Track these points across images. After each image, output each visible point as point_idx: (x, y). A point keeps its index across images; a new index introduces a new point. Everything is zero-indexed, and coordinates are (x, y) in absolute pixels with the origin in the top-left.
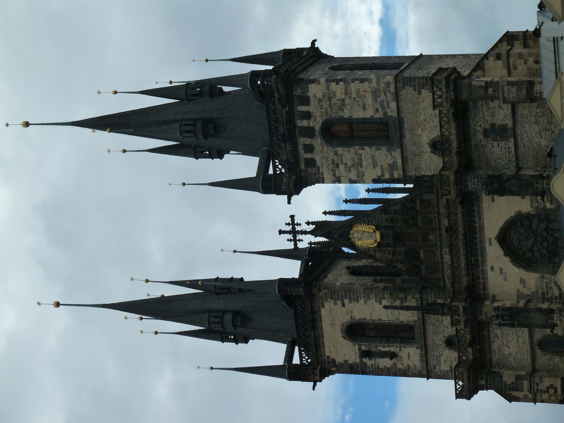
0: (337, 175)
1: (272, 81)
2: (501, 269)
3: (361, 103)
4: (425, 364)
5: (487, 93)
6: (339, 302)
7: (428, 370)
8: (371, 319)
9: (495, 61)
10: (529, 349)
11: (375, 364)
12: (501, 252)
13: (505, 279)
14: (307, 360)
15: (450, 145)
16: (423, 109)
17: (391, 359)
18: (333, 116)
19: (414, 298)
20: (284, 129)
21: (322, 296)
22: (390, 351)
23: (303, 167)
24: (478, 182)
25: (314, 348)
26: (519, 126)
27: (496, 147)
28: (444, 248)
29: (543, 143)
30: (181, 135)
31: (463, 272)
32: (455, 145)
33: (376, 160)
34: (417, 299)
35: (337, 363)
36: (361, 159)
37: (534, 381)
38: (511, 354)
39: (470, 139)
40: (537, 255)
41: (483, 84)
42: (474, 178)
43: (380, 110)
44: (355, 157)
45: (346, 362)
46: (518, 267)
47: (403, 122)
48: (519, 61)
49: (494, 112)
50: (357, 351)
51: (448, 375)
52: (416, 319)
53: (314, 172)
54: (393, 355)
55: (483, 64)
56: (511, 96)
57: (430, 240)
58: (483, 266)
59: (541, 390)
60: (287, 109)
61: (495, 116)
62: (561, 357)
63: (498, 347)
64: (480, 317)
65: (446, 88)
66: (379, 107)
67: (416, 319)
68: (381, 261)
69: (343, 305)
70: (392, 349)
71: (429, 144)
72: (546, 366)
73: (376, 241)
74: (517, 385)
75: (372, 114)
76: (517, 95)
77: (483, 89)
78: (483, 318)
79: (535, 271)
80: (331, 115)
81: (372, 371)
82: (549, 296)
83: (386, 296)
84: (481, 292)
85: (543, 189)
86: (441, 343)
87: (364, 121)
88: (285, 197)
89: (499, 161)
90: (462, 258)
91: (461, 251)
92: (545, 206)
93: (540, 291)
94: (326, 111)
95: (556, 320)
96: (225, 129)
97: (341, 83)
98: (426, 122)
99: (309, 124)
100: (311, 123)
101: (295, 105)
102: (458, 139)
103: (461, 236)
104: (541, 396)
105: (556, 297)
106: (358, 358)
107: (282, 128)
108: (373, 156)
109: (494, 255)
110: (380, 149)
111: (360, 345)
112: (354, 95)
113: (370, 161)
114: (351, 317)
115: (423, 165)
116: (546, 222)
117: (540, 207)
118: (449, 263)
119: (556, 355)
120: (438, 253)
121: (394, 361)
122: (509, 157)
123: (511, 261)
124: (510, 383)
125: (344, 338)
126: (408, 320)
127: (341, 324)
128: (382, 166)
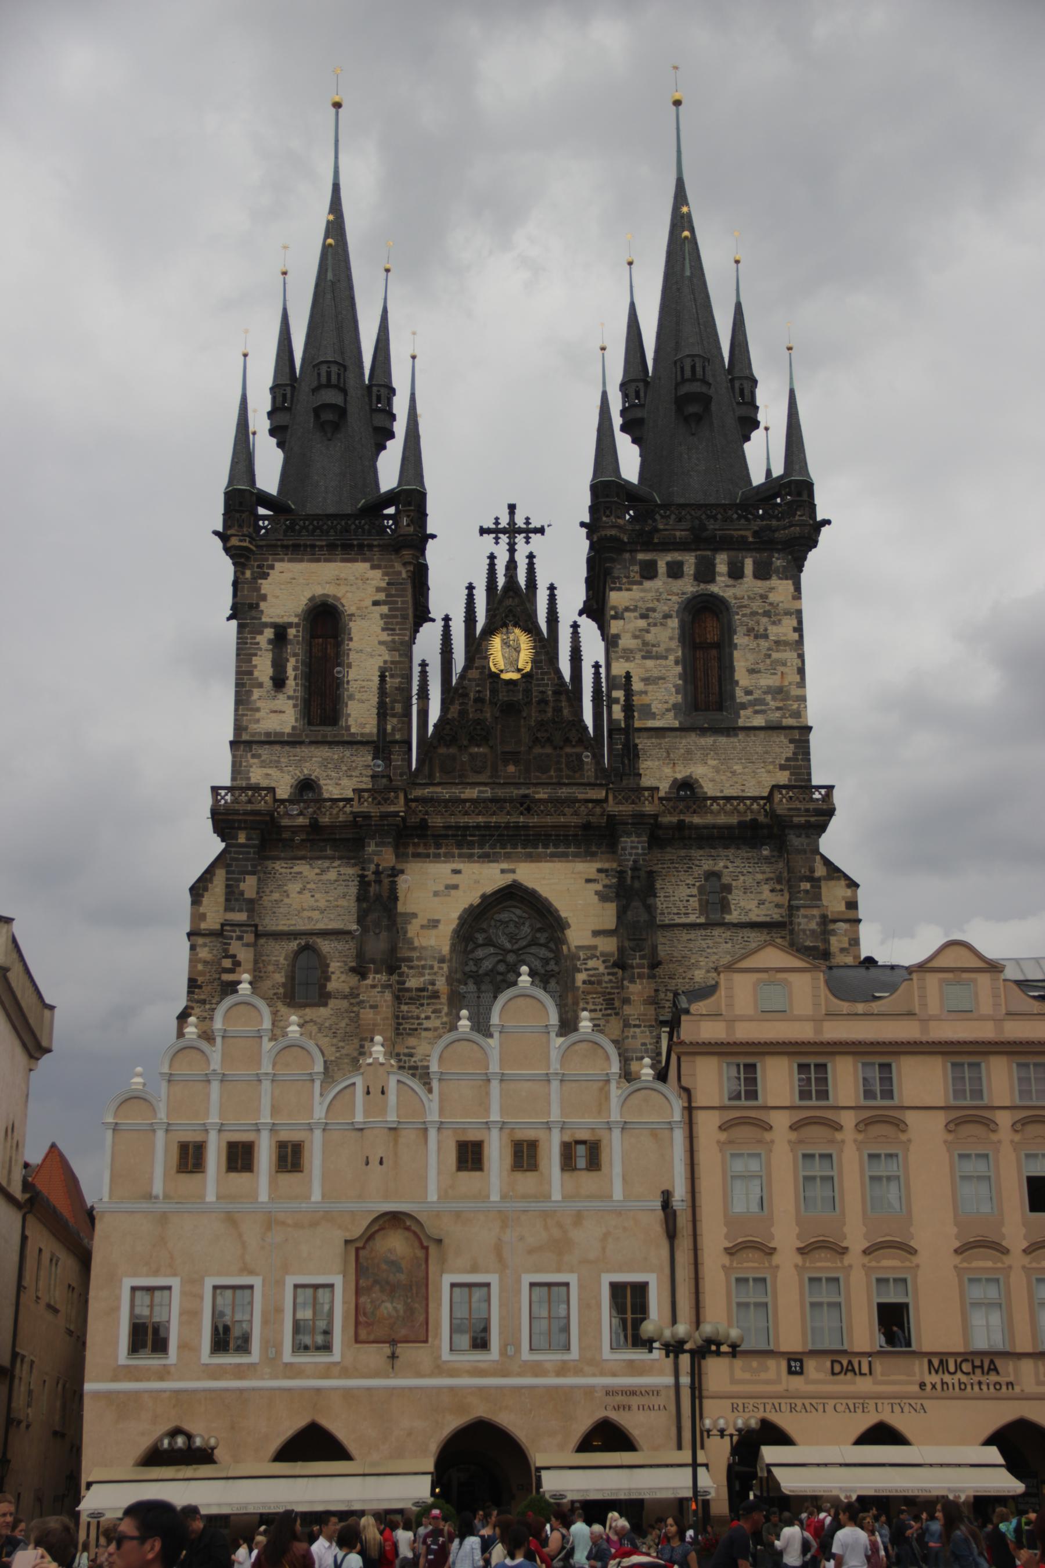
0: (626, 614)
1: (804, 518)
2: (455, 887)
3: (761, 666)
4: (263, 738)
6: (382, 596)
7: (249, 744)
8: (350, 650)
9: (844, 898)
10: (298, 928)
11: (260, 649)
12: (489, 889)
13: (436, 894)
14: (265, 528)
15: (694, 812)
17: (272, 678)
18: (737, 617)
19: (393, 728)
21: (393, 567)
22: (287, 678)
23: (640, 556)
24: (637, 854)
25: (291, 542)
26: (729, 933)
27: (688, 891)
28: (492, 789)
29: (697, 972)
30: (688, 356)
31: (453, 820)
32: (696, 820)
33: (657, 684)
35: (260, 581)
36: (658, 657)
37: (247, 932)
38: (288, 896)
39: (701, 848)
40: (480, 953)
42: (643, 848)
43: (749, 698)
44: (661, 649)
45: (264, 598)
46: (460, 918)
47: (728, 736)
48: (846, 939)
50: (286, 620)
51: (241, 779)
52: (353, 730)
53: (632, 574)
54: (279, 682)
55: (838, 879)
57: (505, 766)
58: (460, 856)
59: (229, 944)
60: (751, 539)
61: (745, 893)
62: (284, 985)
63: (301, 873)
64: (373, 843)
65: (814, 809)
66: (755, 696)
67: (353, 730)
68: (463, 676)
69: (376, 603)
70: (291, 683)
71: (690, 776)
72: (264, 958)
73: (502, 671)
74: (237, 900)
75: (741, 683)
76: (804, 931)
77: (808, 873)
78: (371, 848)
79: (453, 946)
81: (246, 643)
82: (405, 969)
83: (398, 680)
85: (632, 967)
86: (306, 772)
87: (726, 669)
88: (587, 519)
89: (662, 895)
90: (481, 819)
91: (494, 819)
92: (579, 971)
93: (415, 954)
94: (745, 606)
95: (374, 978)
96: (693, 434)
97: (796, 636)
99: (721, 575)
100: (723, 579)
102: (706, 827)
104: (205, 945)
105: (404, 983)
106: (272, 620)
107: (717, 527)
108: (664, 679)
109: (483, 877)
110: (677, 693)
111: (297, 625)
112: (775, 655)
113: (656, 673)
114: (353, 615)
115: (649, 763)
116: (543, 971)
118: (463, 796)
119: (286, 977)
120: (482, 778)
121: (268, 683)
122: (669, 913)
123: (471, 905)
124: (241, 888)
125: (312, 599)
126: (349, 715)
127: (339, 595)
128: (646, 693)
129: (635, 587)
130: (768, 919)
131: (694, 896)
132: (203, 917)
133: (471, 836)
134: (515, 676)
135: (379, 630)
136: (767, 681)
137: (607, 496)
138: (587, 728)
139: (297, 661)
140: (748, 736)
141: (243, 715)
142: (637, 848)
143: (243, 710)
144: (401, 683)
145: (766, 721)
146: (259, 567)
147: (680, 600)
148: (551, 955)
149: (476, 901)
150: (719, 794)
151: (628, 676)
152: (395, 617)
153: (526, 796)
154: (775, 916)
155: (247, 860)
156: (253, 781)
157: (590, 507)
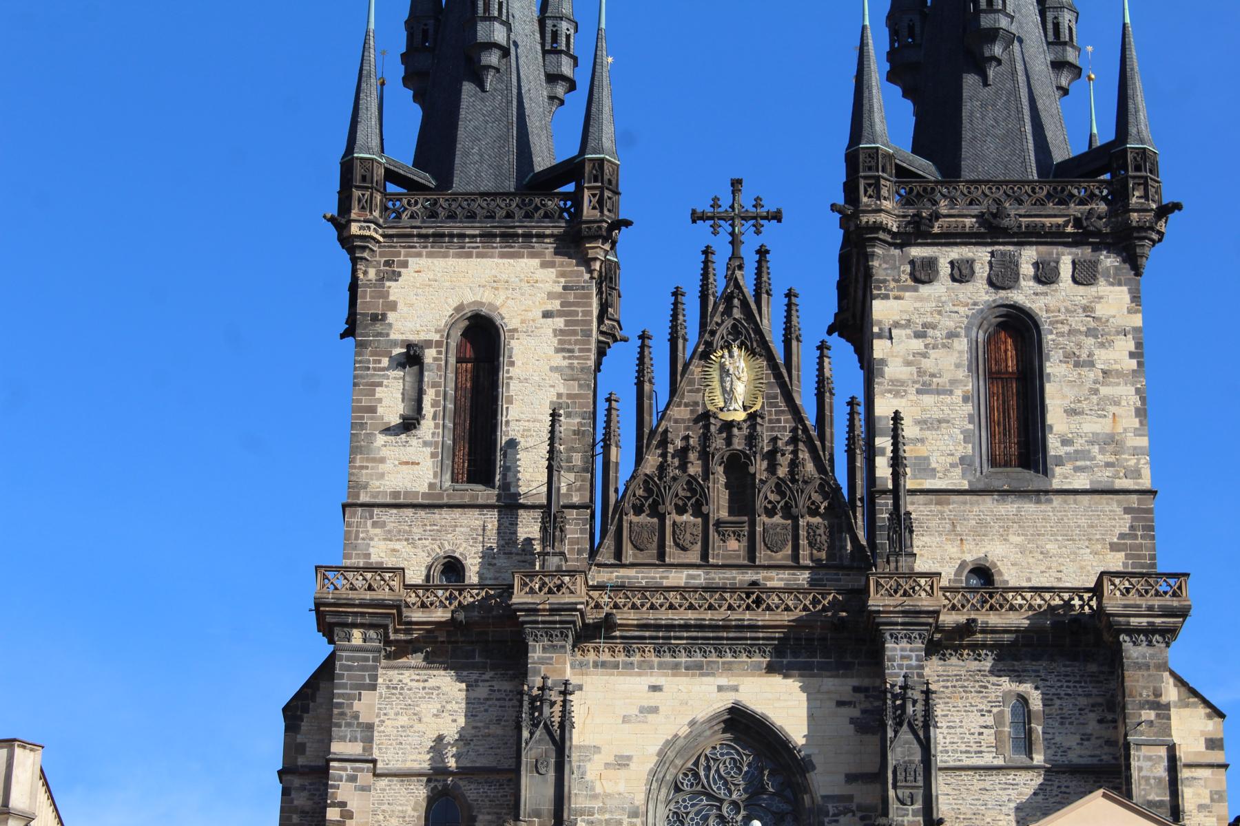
2: (654, 710)
3: (1085, 405)
4: (388, 500)
5: (1142, 708)
6: (555, 305)
8: (510, 378)
13: (626, 719)
15: (992, 608)
16: (1075, 553)
18: (1050, 337)
20: (1021, 216)
23: (916, 252)
25: (431, 231)
28: (707, 573)
31: (651, 617)
32: (994, 620)
34: (568, 495)
35: (388, 284)
36: (938, 392)
37: (362, 770)
41: (1164, 700)
44: (943, 381)
45: (393, 306)
47: (1039, 502)
48: (1208, 792)
49: (1071, 723)
50: (423, 336)
54: (409, 424)
55: (1194, 705)
56: (1146, 765)
60: (1069, 229)
64: (539, 646)
66: (1077, 447)
69: (547, 315)
70: (427, 427)
73: (721, 409)
74: (349, 725)
75: (1055, 429)
76: (1147, 779)
77: (1152, 698)
80: (1051, 333)
81: (368, 368)
84: (591, 657)
86: (447, 547)
90: (691, 616)
93: (597, 804)
97: (1133, 364)
98: (1041, 557)
101: (1074, 250)
103: (747, 615)
104: (303, 788)
107: (1022, 212)
111: (438, 344)
112: (1104, 391)
113: (937, 415)
114: (515, 330)
117: (826, 820)
118: (666, 583)
122: (954, 751)
125: (459, 309)
127: (498, 304)
128: (922, 441)
129: (907, 294)
130: (1095, 761)
131: (991, 727)
132: (301, 749)
133: (676, 638)
134: (740, 416)
135: (551, 351)
136: (1092, 426)
137: (870, 169)
138: (839, 488)
139: (437, 394)
140: (1065, 502)
141: (362, 468)
142: (909, 658)
143: (362, 460)
144: (581, 424)
145: (1091, 482)
146: (387, 263)
147: (970, 313)
148: (785, 807)
149: (684, 730)
150: (1025, 584)
151: (897, 418)
152: (574, 333)
153: (754, 583)
154: (1104, 757)
155: (363, 669)
156: (374, 559)
157: (845, 184)
